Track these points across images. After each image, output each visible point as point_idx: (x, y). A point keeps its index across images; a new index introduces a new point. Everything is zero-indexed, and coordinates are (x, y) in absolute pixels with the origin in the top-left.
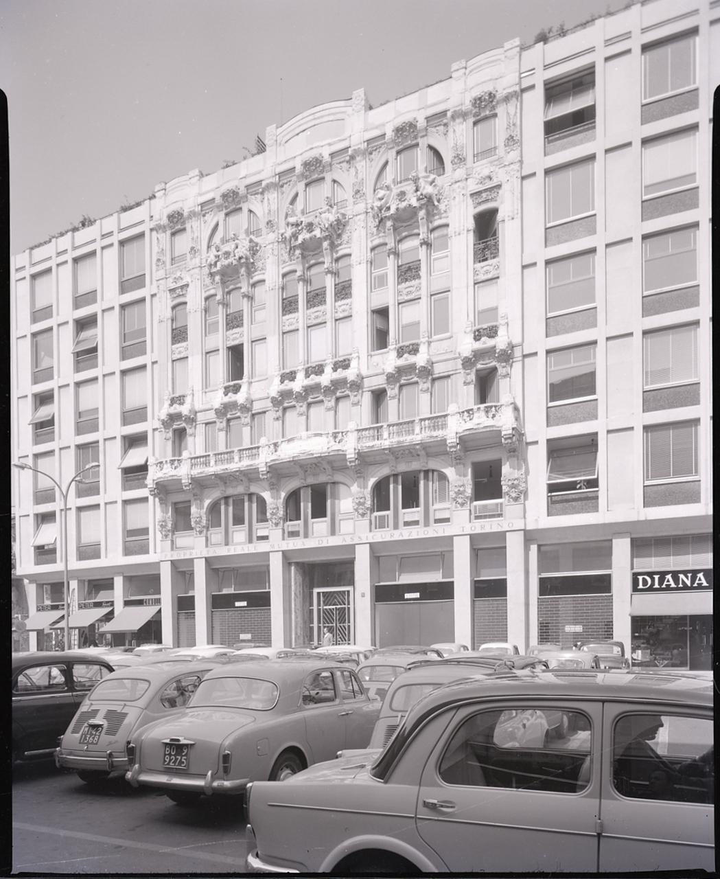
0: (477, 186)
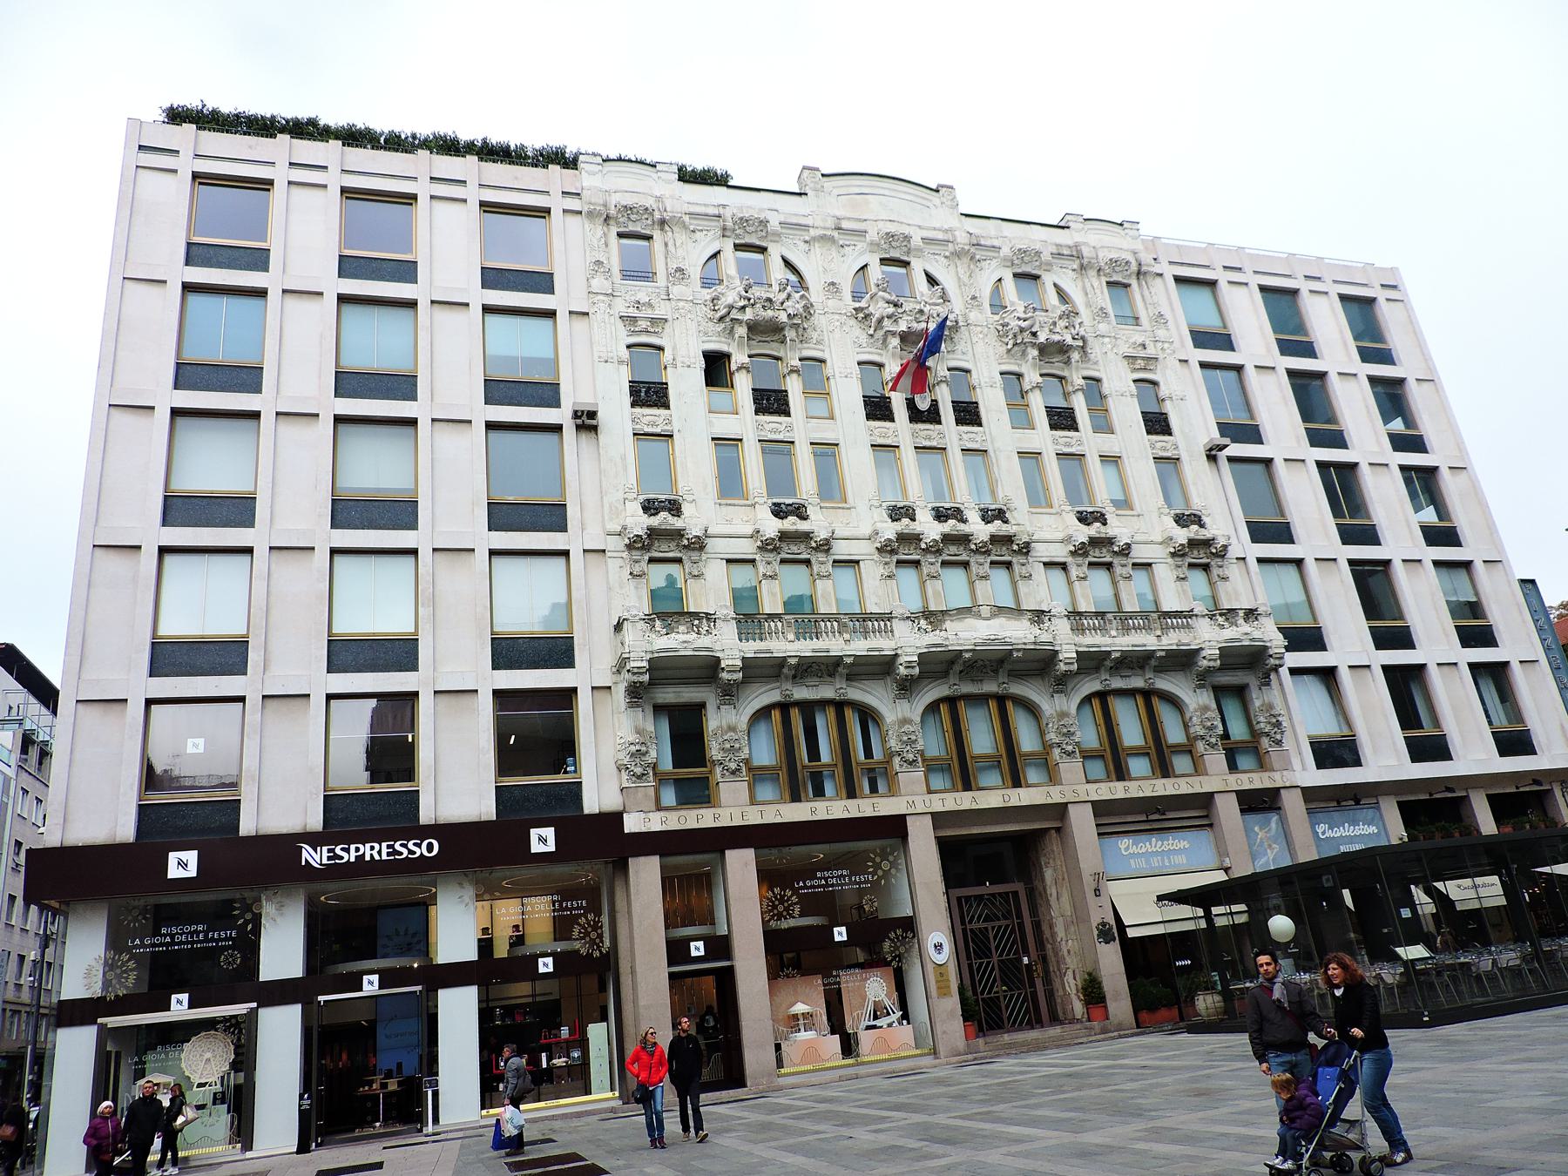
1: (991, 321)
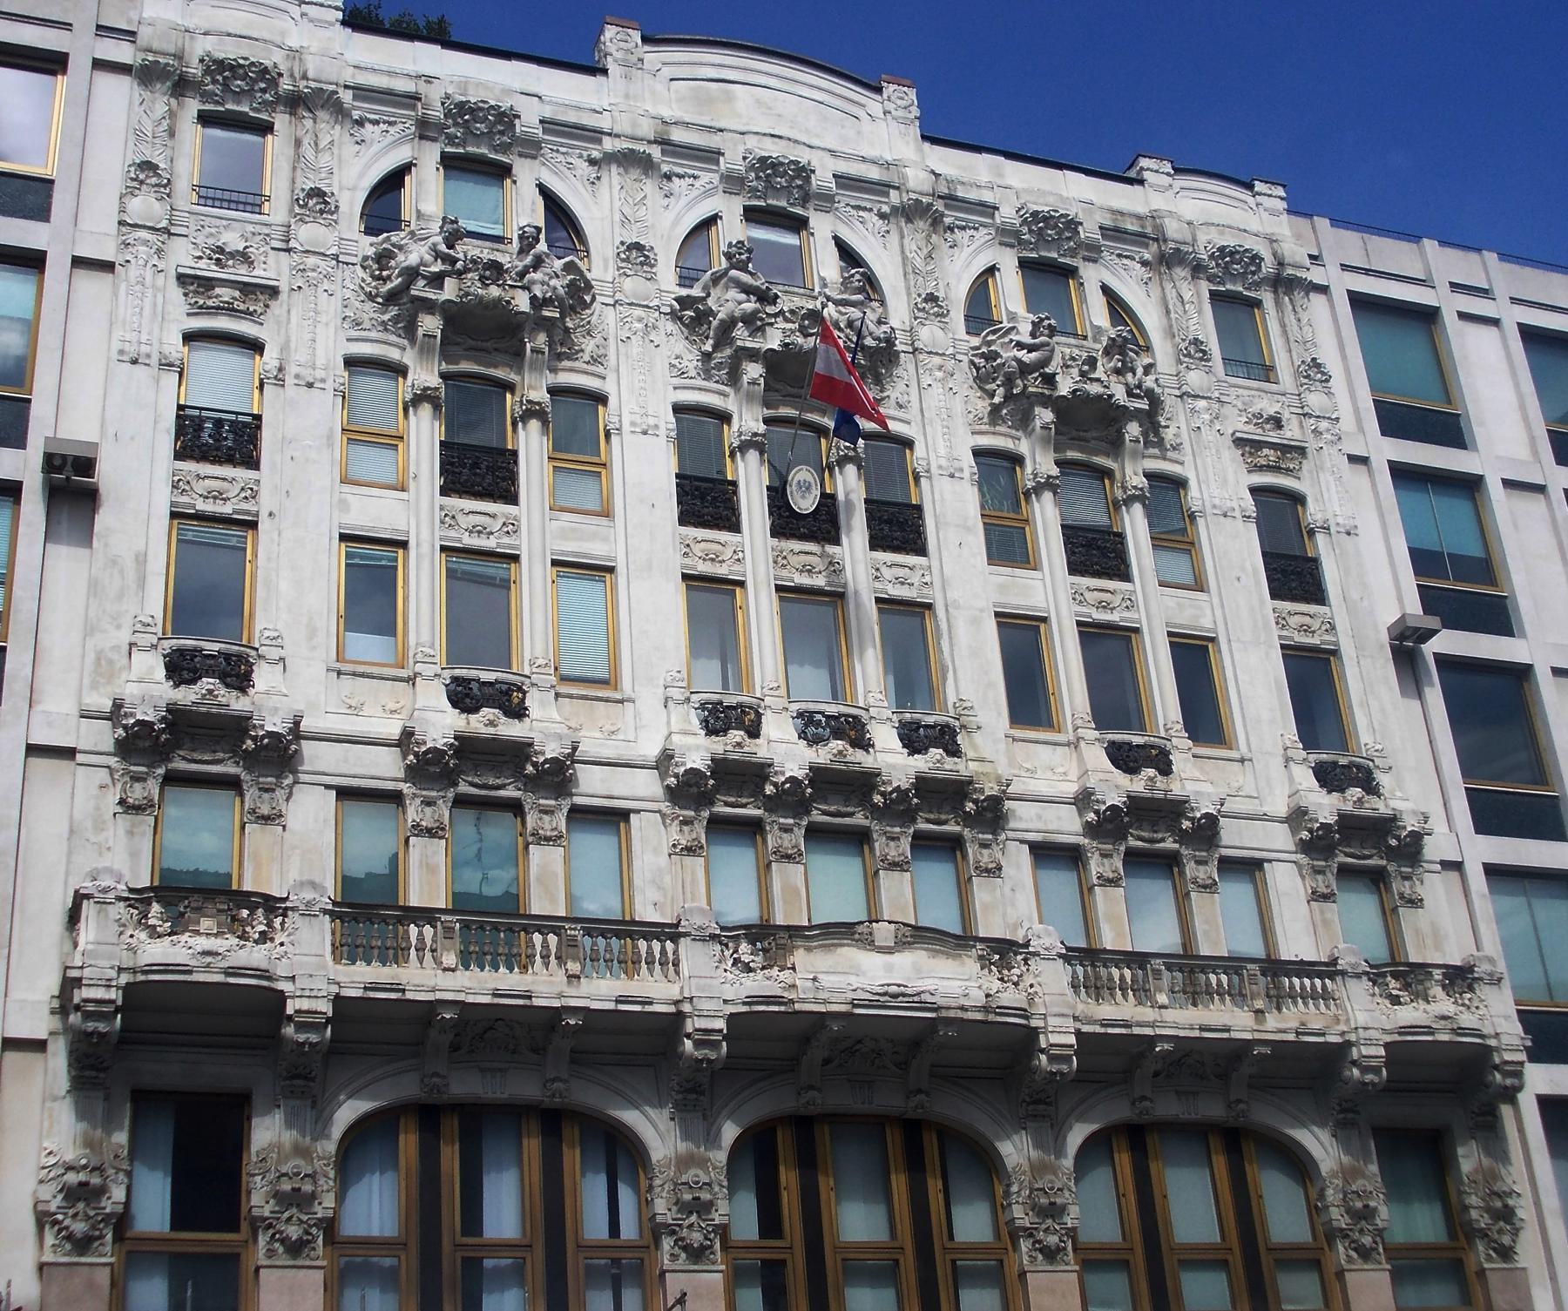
0: (1251, 428)
1: (964, 347)
